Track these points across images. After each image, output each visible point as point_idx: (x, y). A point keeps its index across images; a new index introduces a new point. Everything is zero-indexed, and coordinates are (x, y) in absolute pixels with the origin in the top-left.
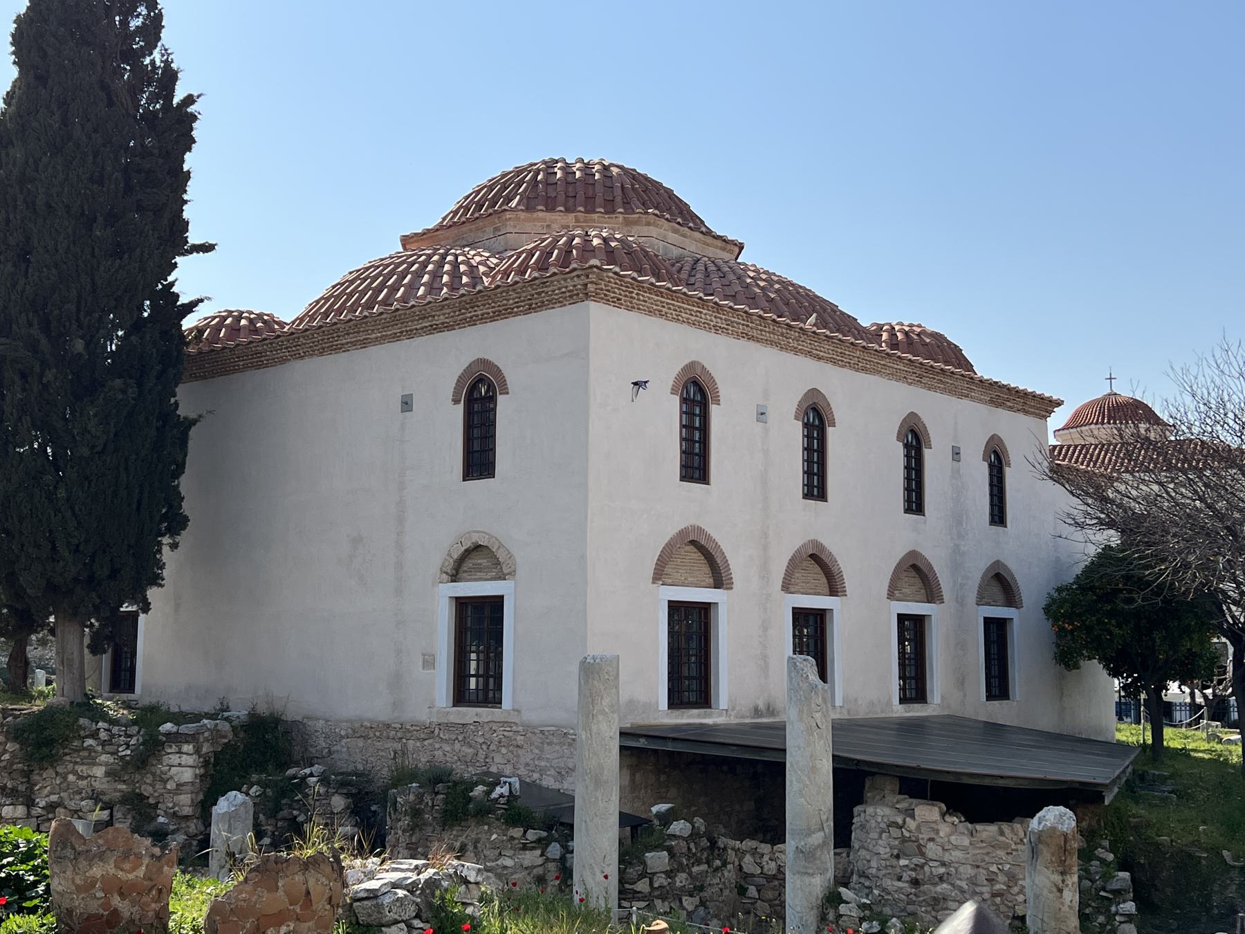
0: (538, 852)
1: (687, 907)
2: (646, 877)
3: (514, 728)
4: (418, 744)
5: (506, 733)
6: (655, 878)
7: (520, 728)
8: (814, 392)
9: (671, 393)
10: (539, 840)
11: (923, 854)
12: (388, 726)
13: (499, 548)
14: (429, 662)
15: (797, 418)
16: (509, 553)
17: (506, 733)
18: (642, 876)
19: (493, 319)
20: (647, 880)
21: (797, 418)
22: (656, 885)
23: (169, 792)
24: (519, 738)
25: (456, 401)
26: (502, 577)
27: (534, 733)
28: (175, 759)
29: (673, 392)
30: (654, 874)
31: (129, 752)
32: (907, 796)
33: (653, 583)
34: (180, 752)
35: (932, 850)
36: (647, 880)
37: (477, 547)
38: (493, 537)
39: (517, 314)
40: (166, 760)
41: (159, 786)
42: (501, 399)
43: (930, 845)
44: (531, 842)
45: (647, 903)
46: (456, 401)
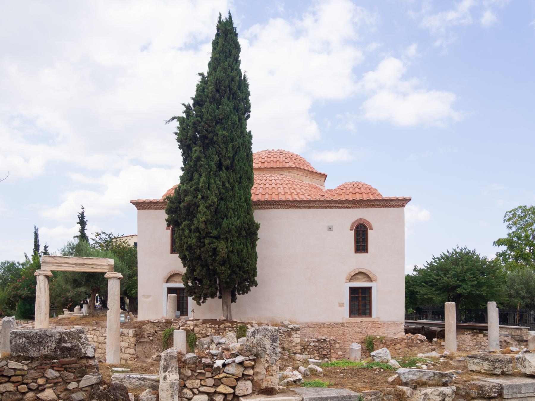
3: (377, 322)
4: (338, 328)
5: (374, 324)
7: (379, 323)
11: (481, 345)
12: (324, 324)
13: (370, 273)
14: (341, 305)
16: (374, 275)
17: (374, 324)
19: (366, 208)
23: (294, 346)
24: (379, 325)
25: (351, 230)
26: (372, 281)
27: (385, 324)
28: (295, 336)
35: (483, 344)
37: (360, 273)
38: (367, 270)
39: (376, 207)
41: (290, 344)
42: (370, 232)
43: (482, 342)
46: (351, 230)
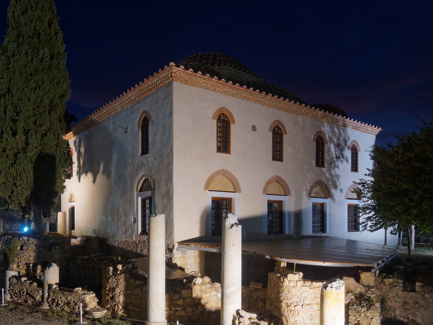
0: (140, 289)
1: (199, 310)
2: (182, 299)
6: (186, 299)
8: (278, 121)
9: (212, 119)
10: (140, 285)
15: (270, 131)
18: (180, 298)
20: (182, 300)
21: (270, 131)
22: (186, 302)
29: (213, 118)
30: (185, 298)
31: (42, 249)
32: (288, 269)
33: (205, 190)
34: (56, 249)
36: (182, 300)
40: (52, 251)
44: (137, 285)
45: (182, 308)
